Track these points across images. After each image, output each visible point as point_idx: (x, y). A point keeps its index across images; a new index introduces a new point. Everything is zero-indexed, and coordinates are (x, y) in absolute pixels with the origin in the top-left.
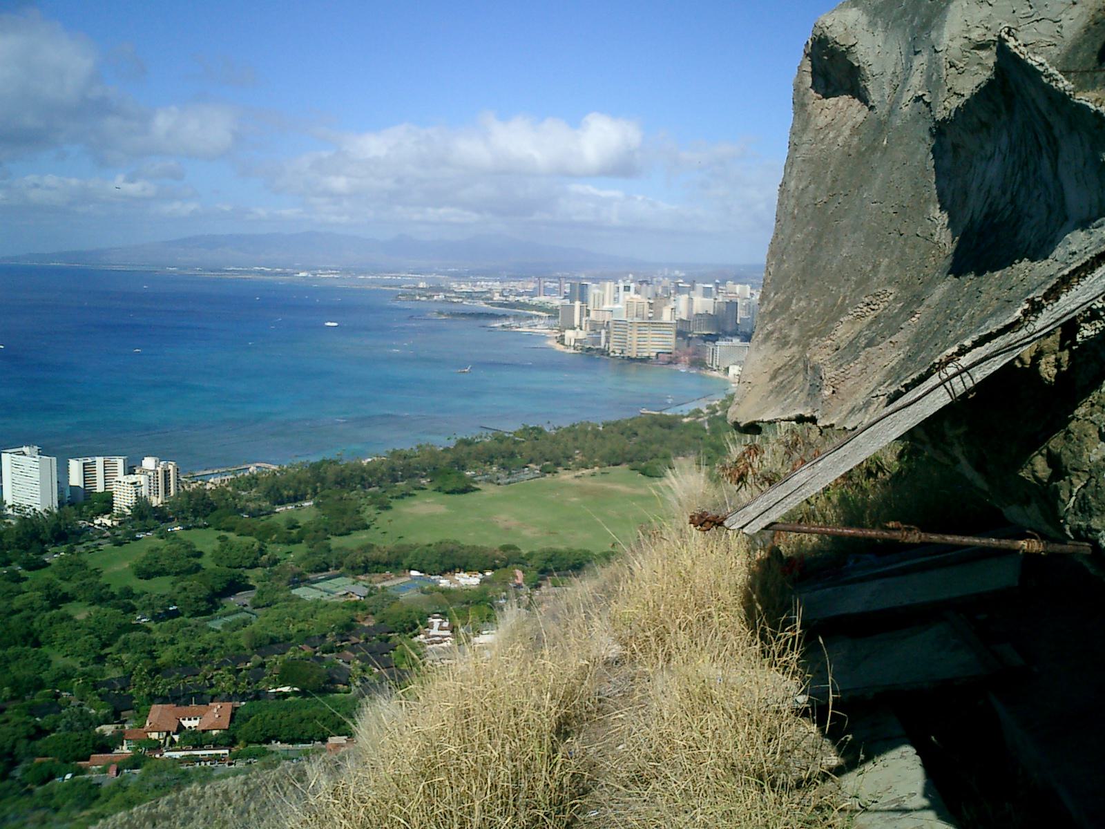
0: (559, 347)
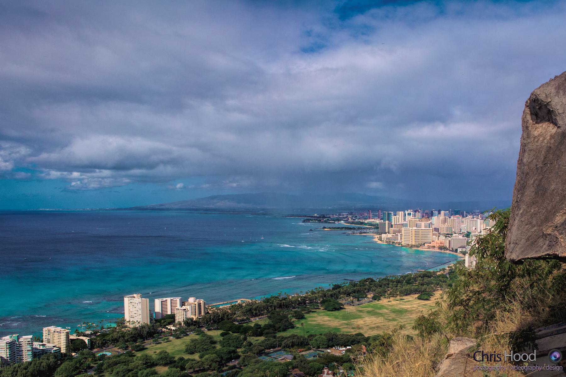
0: (379, 242)
